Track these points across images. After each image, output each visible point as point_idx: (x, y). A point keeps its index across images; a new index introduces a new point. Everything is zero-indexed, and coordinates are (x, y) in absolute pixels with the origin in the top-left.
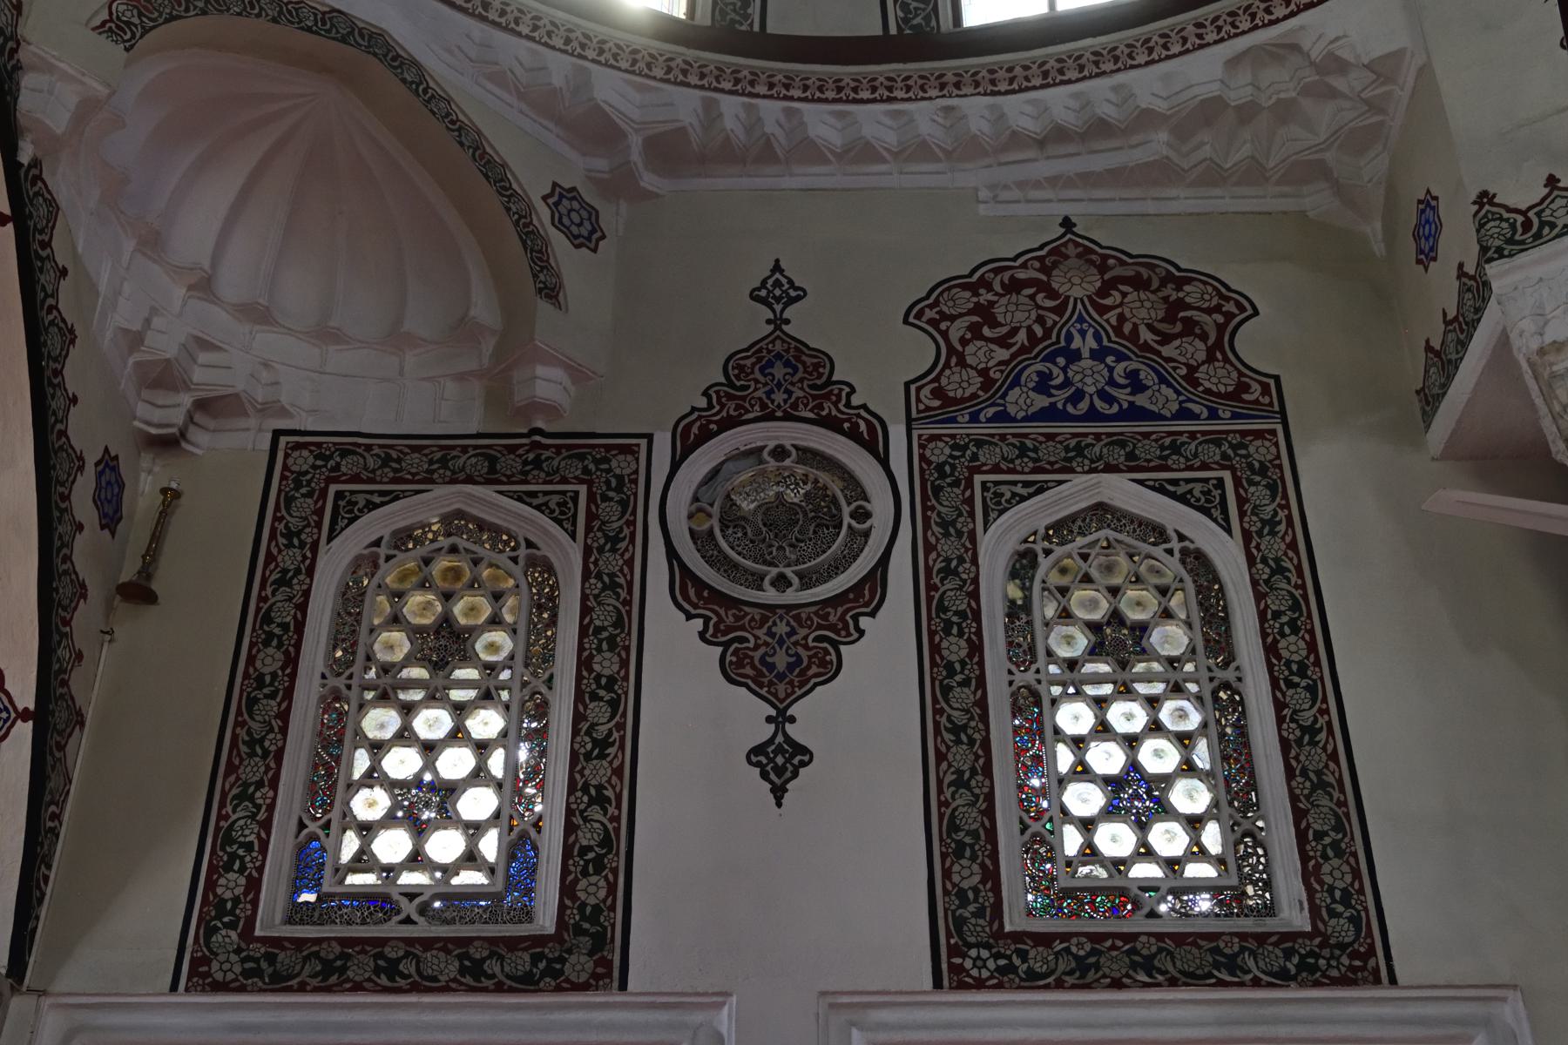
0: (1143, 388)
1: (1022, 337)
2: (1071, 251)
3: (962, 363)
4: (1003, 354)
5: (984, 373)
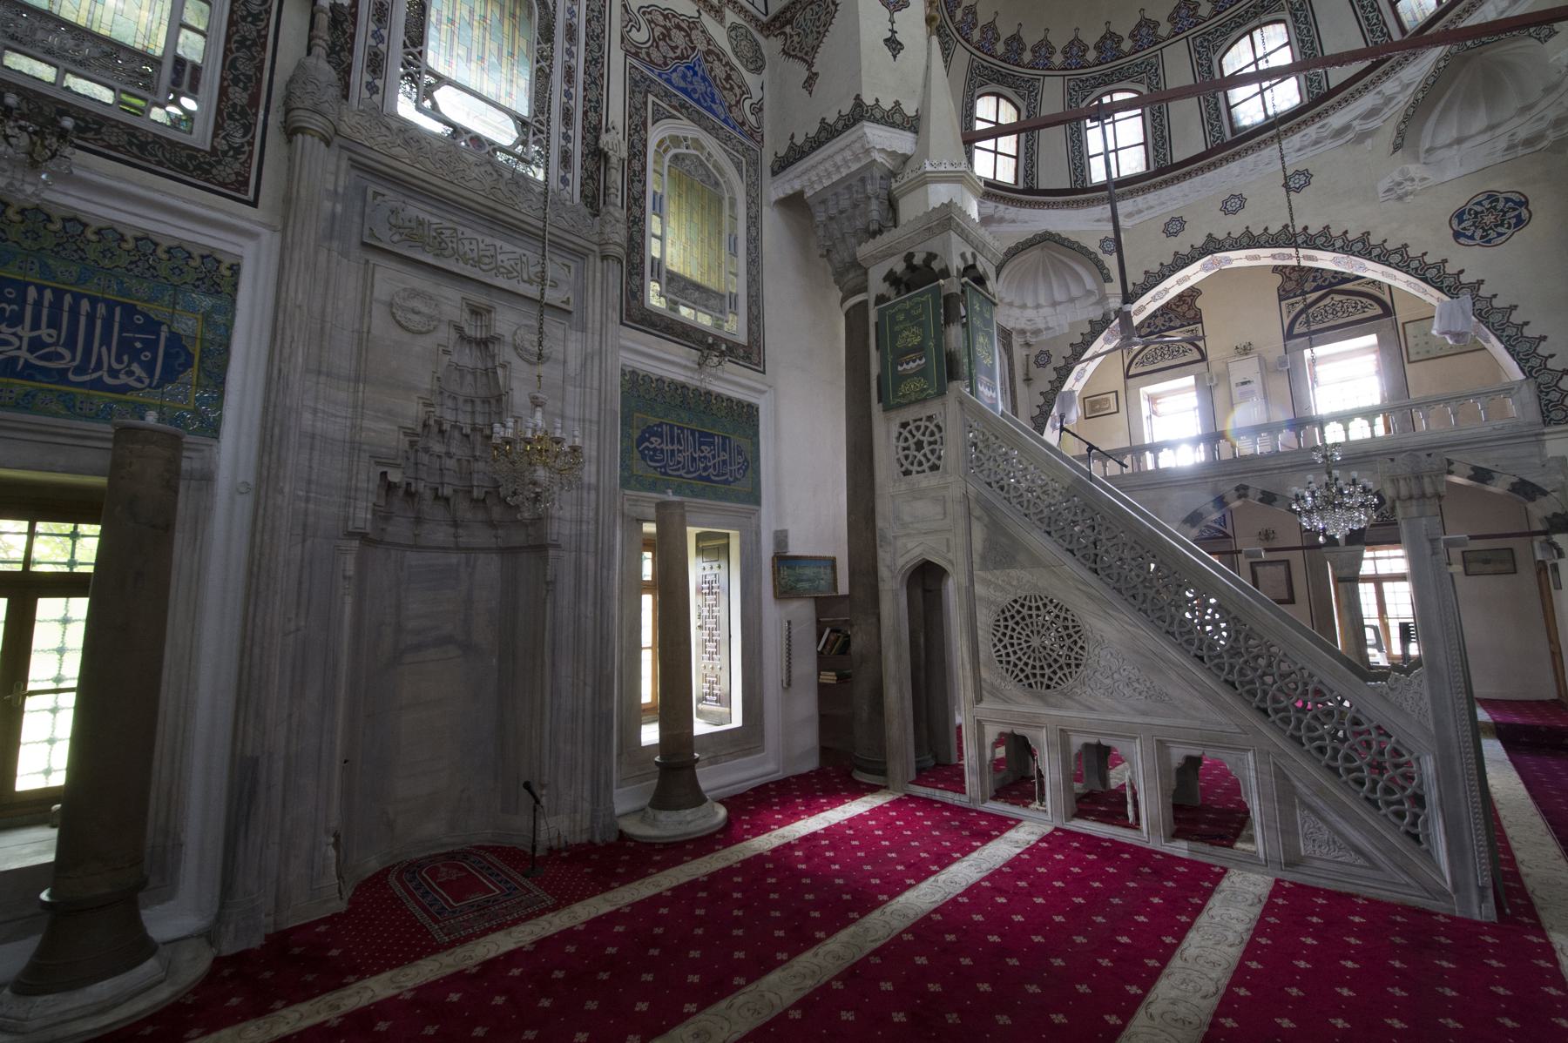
0: (715, 103)
1: (679, 52)
2: (699, 26)
3: (657, 47)
4: (671, 54)
5: (665, 57)
